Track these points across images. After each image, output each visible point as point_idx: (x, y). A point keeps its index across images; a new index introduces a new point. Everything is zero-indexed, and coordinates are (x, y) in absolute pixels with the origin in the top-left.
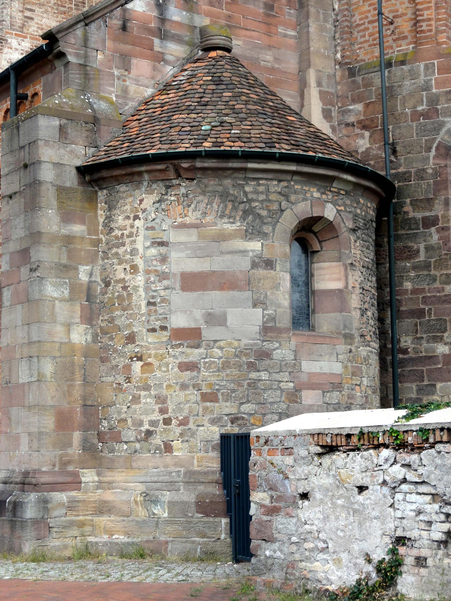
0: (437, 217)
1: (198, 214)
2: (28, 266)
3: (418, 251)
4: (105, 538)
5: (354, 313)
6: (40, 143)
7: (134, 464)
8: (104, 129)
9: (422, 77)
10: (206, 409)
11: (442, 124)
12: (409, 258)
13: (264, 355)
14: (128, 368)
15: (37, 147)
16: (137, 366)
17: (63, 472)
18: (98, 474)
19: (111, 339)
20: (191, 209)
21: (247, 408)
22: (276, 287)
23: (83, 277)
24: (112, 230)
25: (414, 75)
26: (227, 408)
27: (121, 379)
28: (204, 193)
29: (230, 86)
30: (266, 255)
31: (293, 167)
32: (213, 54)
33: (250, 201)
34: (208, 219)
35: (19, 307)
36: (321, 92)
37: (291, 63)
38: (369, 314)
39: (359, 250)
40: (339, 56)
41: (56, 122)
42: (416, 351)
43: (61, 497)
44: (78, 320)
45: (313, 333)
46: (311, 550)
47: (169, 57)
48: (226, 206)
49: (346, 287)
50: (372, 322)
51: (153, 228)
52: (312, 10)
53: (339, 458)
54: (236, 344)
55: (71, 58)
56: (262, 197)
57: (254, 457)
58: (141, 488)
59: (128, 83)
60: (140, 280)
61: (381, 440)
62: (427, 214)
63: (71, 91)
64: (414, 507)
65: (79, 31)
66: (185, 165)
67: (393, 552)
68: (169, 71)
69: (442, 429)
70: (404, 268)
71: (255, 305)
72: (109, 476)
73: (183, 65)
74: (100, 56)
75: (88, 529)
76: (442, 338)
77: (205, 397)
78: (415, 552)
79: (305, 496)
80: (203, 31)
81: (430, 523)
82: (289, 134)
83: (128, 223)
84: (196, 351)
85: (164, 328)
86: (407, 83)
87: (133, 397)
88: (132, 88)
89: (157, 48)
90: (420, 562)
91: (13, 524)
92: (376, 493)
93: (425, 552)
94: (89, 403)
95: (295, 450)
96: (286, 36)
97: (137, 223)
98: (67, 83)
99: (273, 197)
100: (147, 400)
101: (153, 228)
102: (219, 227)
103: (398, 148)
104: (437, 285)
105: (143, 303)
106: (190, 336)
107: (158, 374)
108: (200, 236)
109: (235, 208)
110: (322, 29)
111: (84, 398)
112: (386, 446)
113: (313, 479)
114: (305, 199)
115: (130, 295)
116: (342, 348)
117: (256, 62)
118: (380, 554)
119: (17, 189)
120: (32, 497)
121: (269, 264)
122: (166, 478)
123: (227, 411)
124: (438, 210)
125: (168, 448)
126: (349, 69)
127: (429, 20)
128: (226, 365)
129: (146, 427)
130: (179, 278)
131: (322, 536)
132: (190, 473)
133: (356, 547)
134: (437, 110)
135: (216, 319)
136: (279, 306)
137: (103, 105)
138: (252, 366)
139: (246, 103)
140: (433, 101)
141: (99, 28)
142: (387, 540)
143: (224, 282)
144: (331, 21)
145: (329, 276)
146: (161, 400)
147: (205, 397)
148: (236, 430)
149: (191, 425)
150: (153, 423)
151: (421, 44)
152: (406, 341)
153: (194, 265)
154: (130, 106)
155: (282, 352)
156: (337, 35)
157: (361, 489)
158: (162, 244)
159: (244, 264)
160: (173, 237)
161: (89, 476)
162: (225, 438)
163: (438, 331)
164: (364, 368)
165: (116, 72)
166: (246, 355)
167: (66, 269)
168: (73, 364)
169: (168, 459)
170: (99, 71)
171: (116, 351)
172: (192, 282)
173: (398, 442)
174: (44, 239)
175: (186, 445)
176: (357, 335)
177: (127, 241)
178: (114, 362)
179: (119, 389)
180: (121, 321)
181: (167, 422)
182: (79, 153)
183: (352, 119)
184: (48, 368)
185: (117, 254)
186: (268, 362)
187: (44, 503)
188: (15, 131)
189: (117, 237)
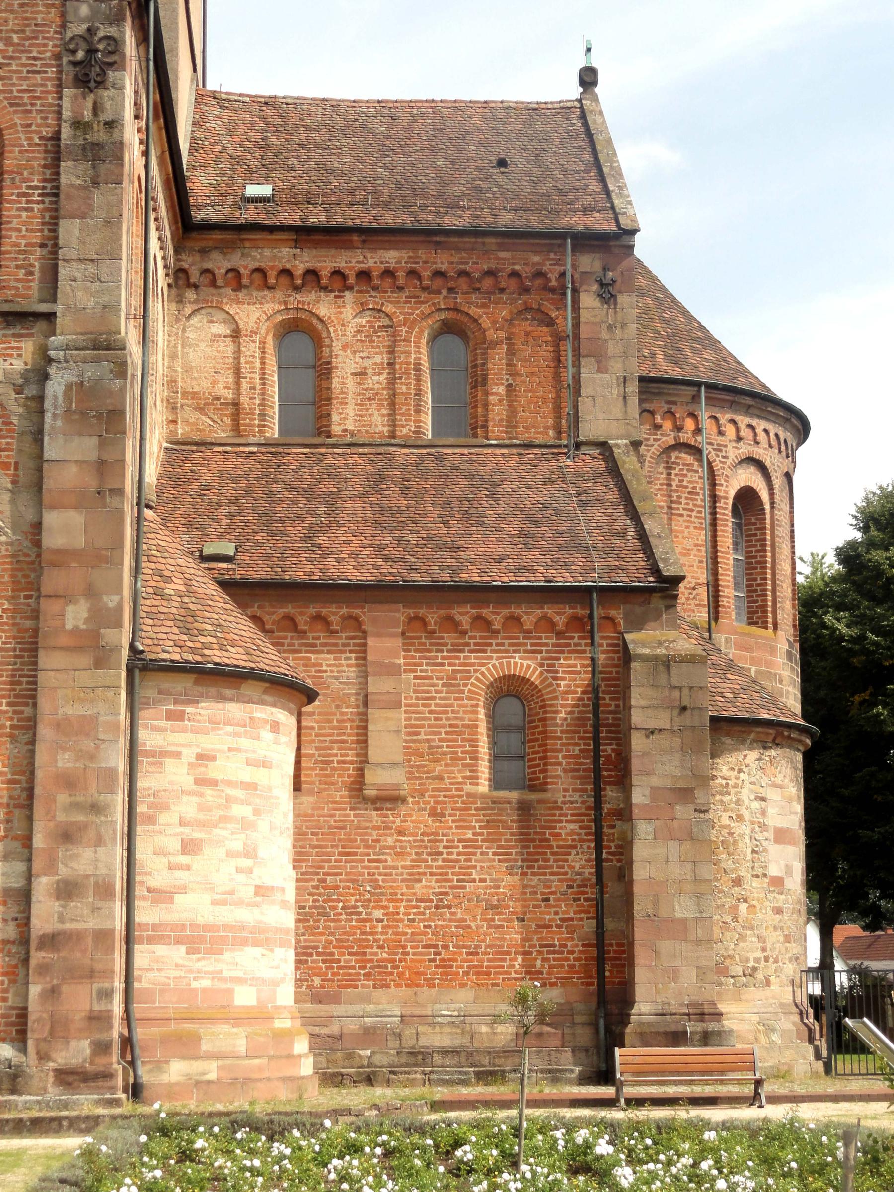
2: (691, 807)
7: (742, 997)
10: (786, 948)
14: (735, 908)
16: (743, 907)
58: (756, 1018)
83: (733, 774)
105: (749, 851)
107: (760, 916)
115: (735, 842)
119: (668, 726)
125: (768, 983)
150: (757, 960)
158: (763, 799)
169: (768, 992)
171: (721, 891)
177: (733, 791)
180: (728, 864)
181: (767, 959)
188: (661, 668)
189: (721, 785)
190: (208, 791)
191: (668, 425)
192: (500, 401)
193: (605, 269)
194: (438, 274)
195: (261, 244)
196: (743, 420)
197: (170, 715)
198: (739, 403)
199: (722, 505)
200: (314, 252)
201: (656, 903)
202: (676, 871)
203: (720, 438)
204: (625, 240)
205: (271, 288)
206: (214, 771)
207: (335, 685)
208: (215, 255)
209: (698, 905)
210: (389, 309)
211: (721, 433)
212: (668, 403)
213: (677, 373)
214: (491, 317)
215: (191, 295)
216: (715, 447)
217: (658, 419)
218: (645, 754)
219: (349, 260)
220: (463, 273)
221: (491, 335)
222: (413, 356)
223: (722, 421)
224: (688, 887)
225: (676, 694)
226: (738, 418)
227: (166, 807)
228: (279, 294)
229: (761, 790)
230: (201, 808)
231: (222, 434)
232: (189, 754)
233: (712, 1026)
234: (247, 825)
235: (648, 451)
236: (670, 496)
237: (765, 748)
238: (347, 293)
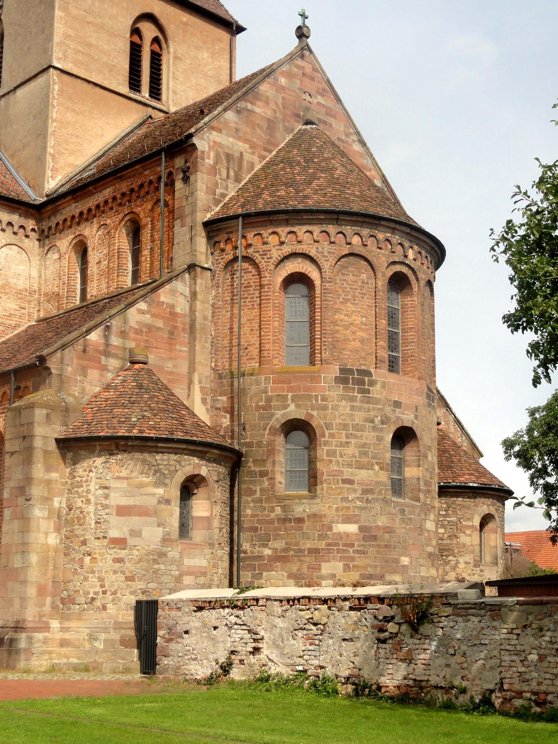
0: (268, 471)
1: (128, 471)
2: (24, 497)
3: (256, 491)
4: (65, 660)
5: (215, 530)
6: (35, 424)
7: (83, 617)
8: (71, 414)
9: (263, 385)
10: (128, 585)
11: (273, 415)
12: (250, 495)
13: (163, 555)
14: (81, 560)
15: (33, 426)
16: (87, 559)
17: (40, 621)
18: (60, 623)
19: (72, 542)
20: (124, 468)
21: (152, 585)
22: (171, 515)
23: (56, 504)
24: (74, 477)
25: (258, 383)
26: (140, 585)
27: (77, 566)
28: (132, 459)
29: (148, 391)
30: (166, 497)
31: (184, 446)
32: (137, 366)
33: (158, 465)
34: (134, 474)
35: (16, 522)
36: (201, 387)
37: (184, 368)
38: (224, 530)
39: (220, 493)
40: (213, 364)
41: (45, 412)
42: (252, 552)
43: (39, 636)
44: (52, 530)
45: (191, 542)
46: (189, 659)
47: (110, 368)
48: (144, 468)
49: (211, 515)
50: (225, 535)
51: (100, 478)
52: (198, 336)
53: (205, 613)
54: (147, 548)
55: (53, 371)
56: (165, 463)
57: (160, 612)
58: (88, 631)
59: (85, 385)
60: (91, 508)
61: (226, 604)
62: (262, 469)
63: (52, 391)
64: (239, 636)
65: (59, 354)
66: (122, 443)
67: (229, 658)
68: (110, 376)
69: (253, 599)
70: (247, 501)
71: (159, 526)
72: (67, 624)
73: (118, 372)
74: (70, 369)
75: (54, 655)
76: (267, 545)
77: (127, 579)
78: (239, 657)
80: (131, 351)
81: (246, 643)
82: (183, 425)
84: (123, 551)
85: (105, 537)
86: (254, 387)
87: (84, 577)
88: (88, 387)
89: (103, 363)
90: (241, 662)
91: (10, 652)
92: (223, 629)
93: (243, 657)
94: (56, 580)
95: (182, 609)
96: (180, 351)
97: (91, 474)
98: (50, 386)
99: (172, 463)
100: (93, 580)
101: (100, 478)
102: (140, 479)
103: (246, 427)
104: (266, 512)
105: (93, 522)
106: (120, 543)
107: (100, 564)
108: (128, 485)
109: (149, 469)
110: (203, 347)
111: (54, 577)
112: (228, 607)
113: (191, 623)
114: (190, 464)
115: (84, 517)
116: (207, 551)
117: (161, 368)
118: (222, 660)
120: (23, 635)
121: (168, 502)
122: (102, 626)
123: (140, 587)
125: (104, 608)
126: (219, 374)
127: (269, 350)
128: (140, 560)
129: (92, 595)
130: (115, 508)
131: (195, 652)
132: (116, 623)
133: (211, 657)
134: (271, 406)
136: (172, 526)
137: (70, 400)
138: (155, 561)
139: (157, 403)
140: (269, 400)
141: (70, 352)
142: (226, 652)
143: (142, 512)
144: (209, 341)
145: (200, 507)
146: (101, 579)
147: (127, 579)
148: (145, 598)
149: (119, 595)
150: (96, 593)
151: (263, 364)
152: (246, 546)
153: (124, 501)
154: (86, 398)
155: (173, 553)
156: (213, 352)
157: (215, 628)
158: (106, 488)
159: (154, 501)
160: (113, 484)
161: (55, 624)
162: (139, 603)
163: (266, 540)
164: (220, 563)
165: (79, 378)
166: (153, 555)
167: (47, 500)
168: (48, 557)
170: (69, 377)
171: (74, 549)
172: (122, 511)
173: (232, 605)
174: (35, 482)
175: (115, 606)
176: (216, 544)
177: (85, 484)
178: (73, 556)
179: (75, 572)
180: (79, 532)
181: (104, 592)
182: (59, 430)
183: (219, 406)
185: (77, 491)
186: (164, 559)
187: (31, 638)
188: (18, 414)
189: (78, 482)
191: (229, 248)
192: (146, 259)
193: (186, 162)
194: (123, 194)
195: (64, 205)
196: (283, 231)
198: (275, 220)
199: (266, 290)
200: (82, 202)
201: (8, 559)
202: (17, 538)
203: (265, 246)
204: (190, 143)
205: (70, 227)
208: (52, 218)
209: (23, 559)
210: (108, 221)
211: (265, 243)
212: (228, 233)
213: (240, 211)
214: (142, 210)
215: (47, 242)
216: (261, 253)
217: (222, 245)
218: (10, 468)
219: (91, 202)
220: (132, 190)
221: (144, 221)
222: (117, 245)
223: (265, 235)
225: (22, 428)
226: (279, 230)
228: (73, 229)
229: (106, 482)
231: (55, 312)
233: (16, 636)
235: (218, 267)
236: (232, 292)
237: (111, 455)
238: (95, 220)
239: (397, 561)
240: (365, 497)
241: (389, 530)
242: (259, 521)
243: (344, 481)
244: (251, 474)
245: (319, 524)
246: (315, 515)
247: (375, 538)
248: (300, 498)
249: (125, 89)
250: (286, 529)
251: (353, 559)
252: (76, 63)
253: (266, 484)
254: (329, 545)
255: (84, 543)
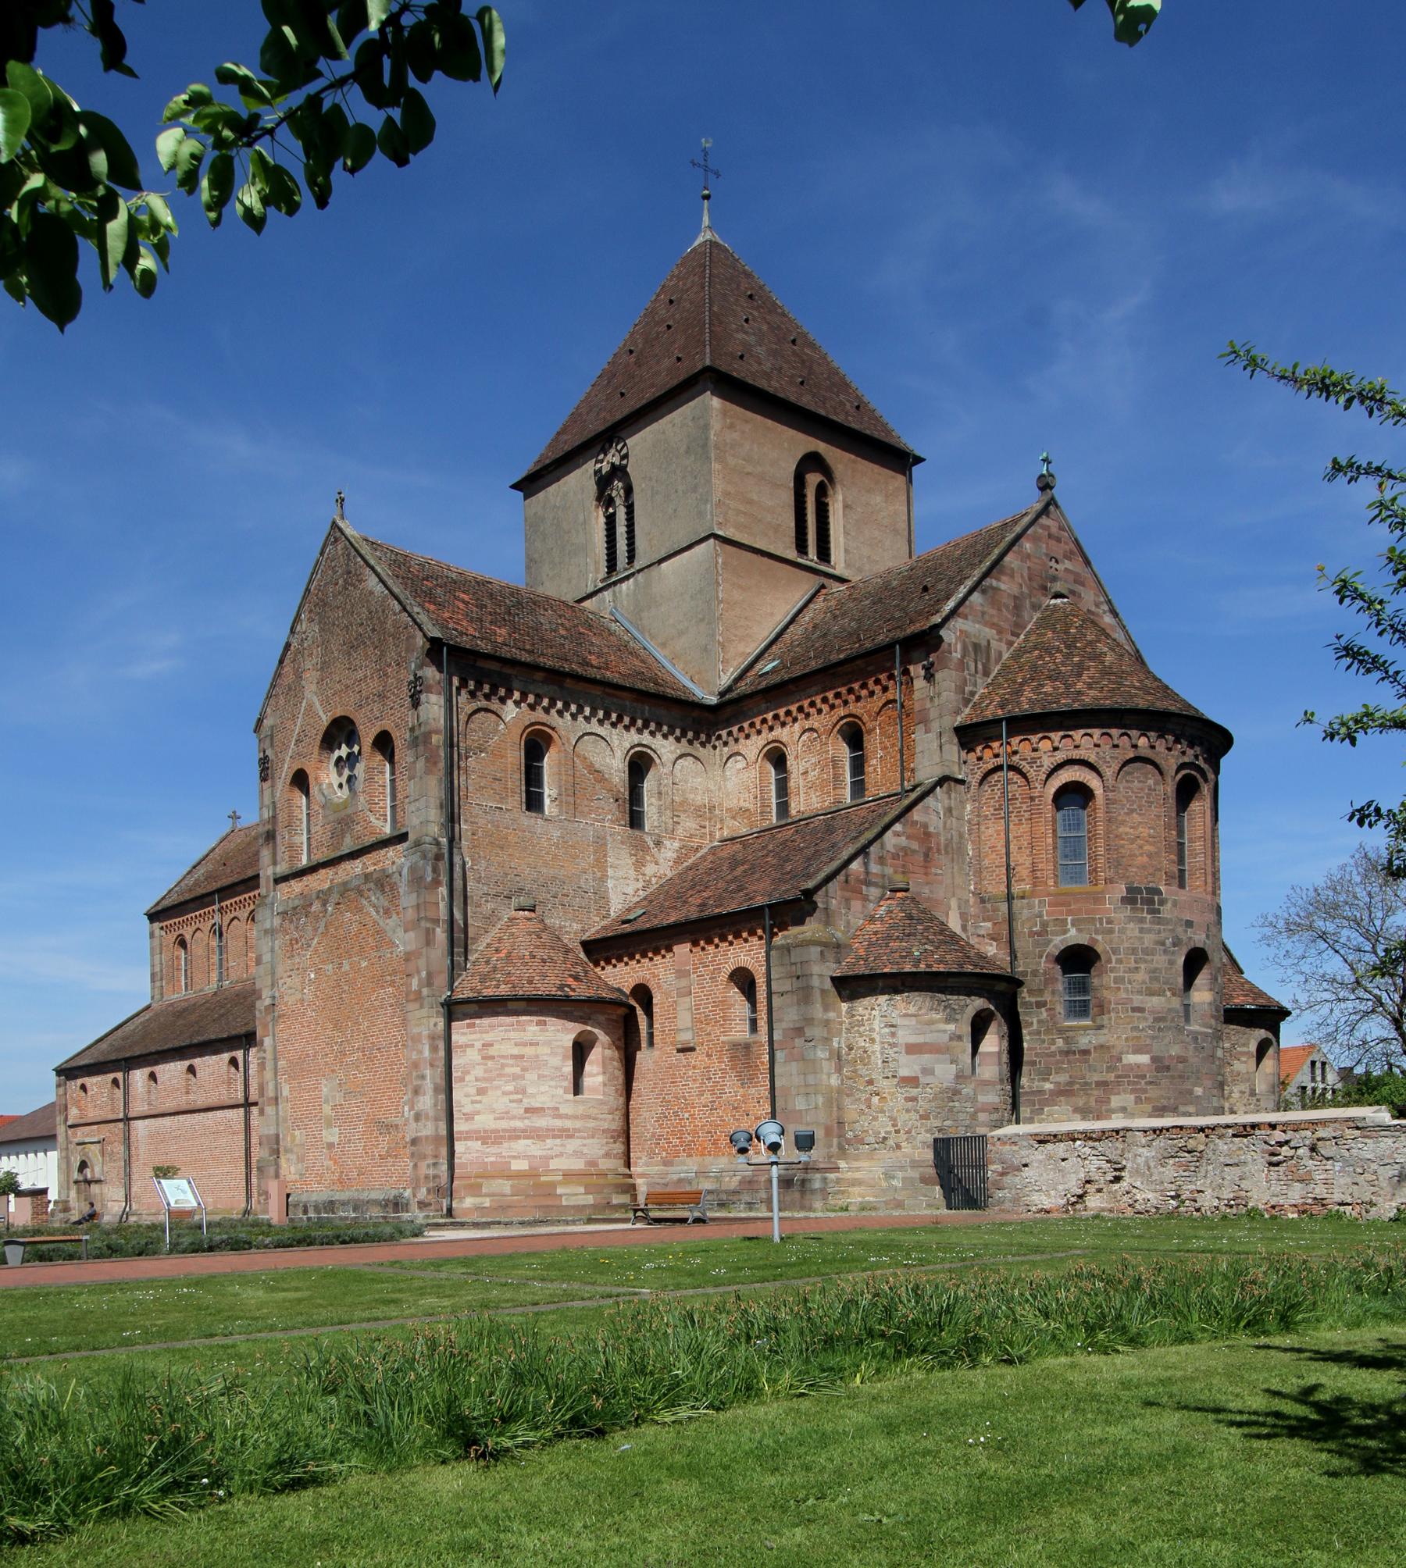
13: (956, 1092)
14: (868, 1100)
16: (875, 1099)
22: (964, 1051)
23: (835, 1044)
35: (794, 1064)
77: (922, 1117)
79: (1025, 1165)
106: (912, 1081)
121: (960, 1038)
124: (1047, 997)
128: (935, 1099)
135: (928, 1071)
146: (893, 1120)
147: (922, 1117)
159: (946, 1037)
172: (912, 1049)
184: (820, 1100)
190: (490, 1063)
197: (469, 1026)
202: (797, 1080)
206: (492, 1052)
207: (665, 986)
224: (802, 1090)
227: (468, 1073)
230: (486, 1071)
232: (478, 1045)
234: (515, 1077)
239: (1191, 1092)
240: (1157, 1025)
241: (1182, 1060)
242: (1037, 1055)
243: (1134, 1010)
244: (1027, 1005)
245: (1107, 1057)
246: (1102, 1046)
247: (1168, 1068)
248: (1085, 1028)
249: (791, 554)
250: (1069, 1062)
251: (1145, 1091)
252: (739, 527)
253: (1044, 1015)
254: (1119, 1076)
255: (870, 1082)
